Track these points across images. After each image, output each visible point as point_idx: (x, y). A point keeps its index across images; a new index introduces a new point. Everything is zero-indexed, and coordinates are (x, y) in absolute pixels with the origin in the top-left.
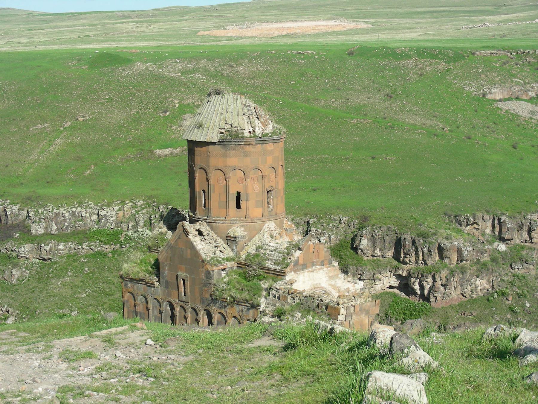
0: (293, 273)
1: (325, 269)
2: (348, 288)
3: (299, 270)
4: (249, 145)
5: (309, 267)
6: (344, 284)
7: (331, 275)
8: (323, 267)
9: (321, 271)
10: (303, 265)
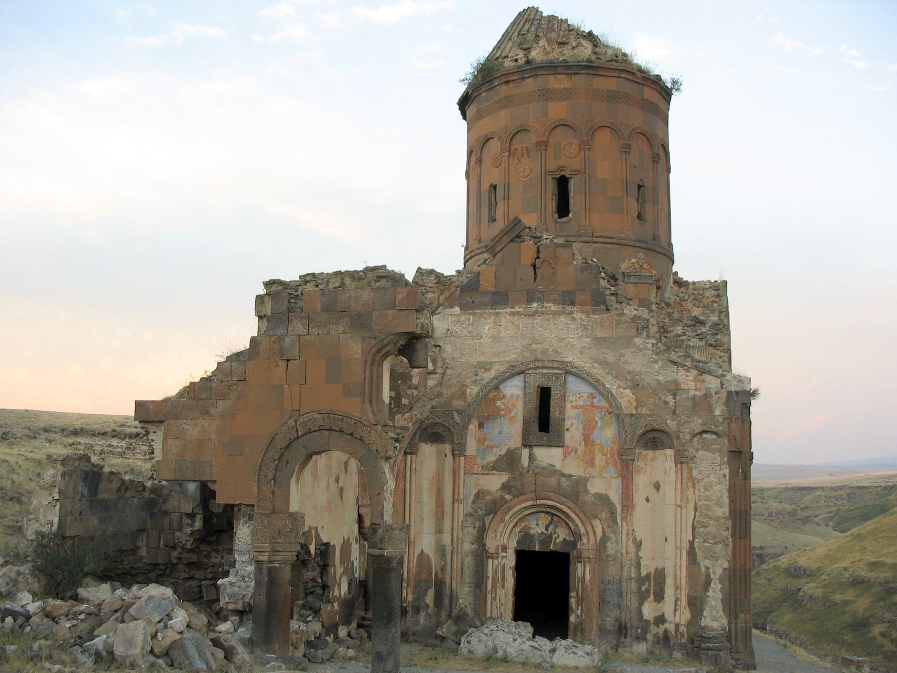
0: (457, 309)
1: (578, 315)
2: (676, 383)
3: (483, 305)
4: (508, 82)
5: (518, 302)
6: (656, 367)
7: (600, 334)
8: (569, 308)
9: (563, 318)
10: (494, 293)
